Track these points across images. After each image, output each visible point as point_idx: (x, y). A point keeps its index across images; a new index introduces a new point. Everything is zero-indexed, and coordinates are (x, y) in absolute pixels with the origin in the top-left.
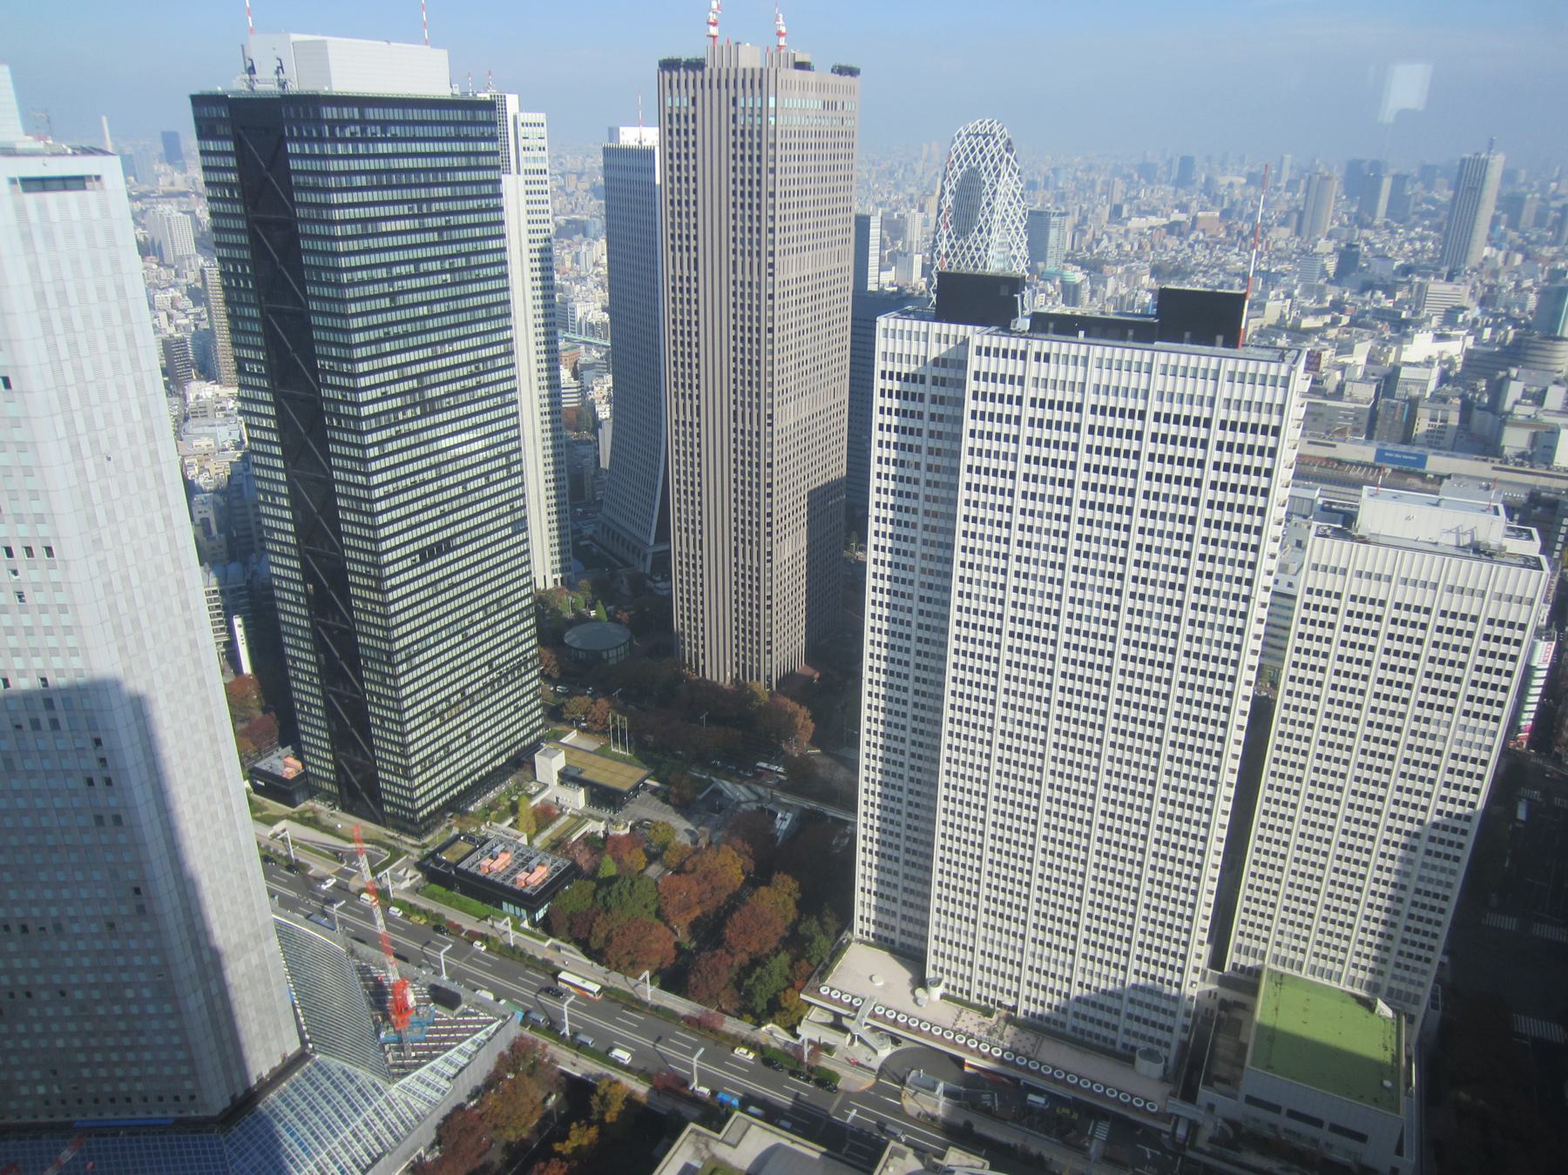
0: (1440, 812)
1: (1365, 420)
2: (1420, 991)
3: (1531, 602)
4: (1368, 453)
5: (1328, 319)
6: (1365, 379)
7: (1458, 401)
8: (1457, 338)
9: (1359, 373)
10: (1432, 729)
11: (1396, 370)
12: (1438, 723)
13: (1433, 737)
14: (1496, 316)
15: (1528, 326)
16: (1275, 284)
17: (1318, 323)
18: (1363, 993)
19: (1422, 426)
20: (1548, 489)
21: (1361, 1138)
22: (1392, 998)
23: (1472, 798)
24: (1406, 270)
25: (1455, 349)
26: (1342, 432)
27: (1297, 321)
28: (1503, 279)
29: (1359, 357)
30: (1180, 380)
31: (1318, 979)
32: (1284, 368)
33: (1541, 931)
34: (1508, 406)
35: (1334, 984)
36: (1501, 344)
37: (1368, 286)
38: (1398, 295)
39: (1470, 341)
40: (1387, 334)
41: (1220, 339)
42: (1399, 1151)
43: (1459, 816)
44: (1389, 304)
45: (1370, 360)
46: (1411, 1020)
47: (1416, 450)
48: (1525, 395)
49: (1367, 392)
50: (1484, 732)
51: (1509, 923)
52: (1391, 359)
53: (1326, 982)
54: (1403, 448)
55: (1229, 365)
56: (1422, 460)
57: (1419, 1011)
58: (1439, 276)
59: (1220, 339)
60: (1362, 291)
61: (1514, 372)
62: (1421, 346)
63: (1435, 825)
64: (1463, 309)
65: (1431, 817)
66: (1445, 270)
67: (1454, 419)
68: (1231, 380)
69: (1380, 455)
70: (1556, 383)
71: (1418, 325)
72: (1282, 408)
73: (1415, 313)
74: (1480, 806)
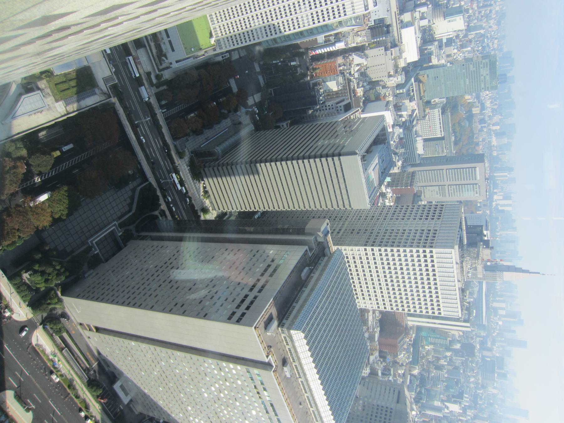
0: (278, 23)
2: (224, 48)
3: (354, 13)
10: (302, 7)
12: (305, 7)
13: (300, 9)
15: (447, 7)
18: (213, 34)
20: (393, 29)
21: (173, 50)
22: (218, 41)
23: (287, 30)
31: (209, 18)
33: (260, 78)
34: (418, 10)
35: (210, 24)
42: (177, 62)
43: (280, 29)
46: (214, 50)
48: (423, 13)
50: (308, 22)
51: (258, 69)
53: (210, 21)
57: (218, 51)
61: (430, 6)
63: (274, 25)
65: (275, 22)
70: (429, 21)
74: (286, 33)
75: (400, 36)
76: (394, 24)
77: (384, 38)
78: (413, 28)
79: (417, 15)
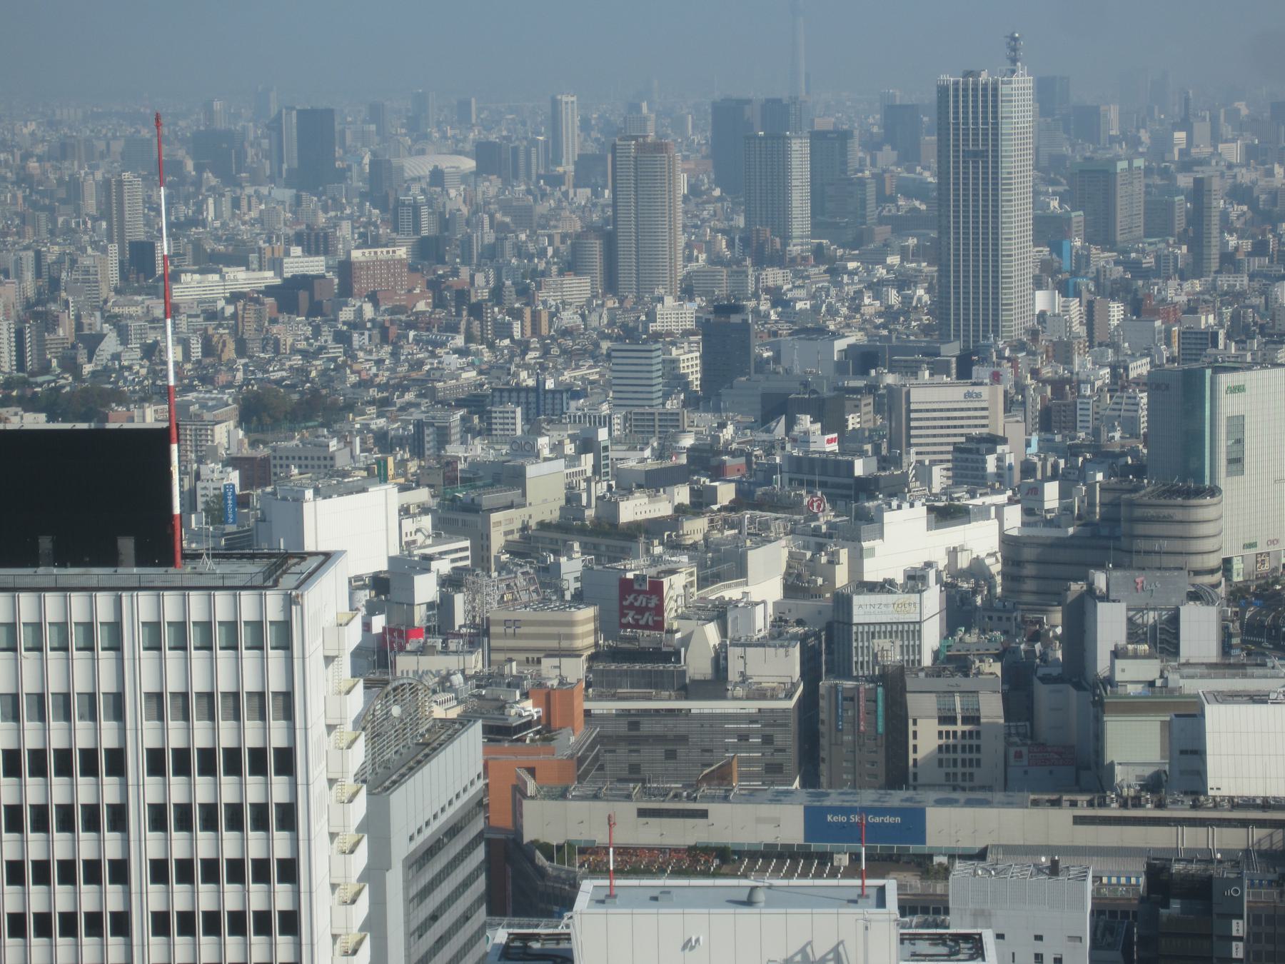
1: (788, 739)
4: (785, 823)
5: (682, 494)
6: (778, 633)
7: (997, 668)
8: (983, 513)
9: (761, 622)
11: (843, 603)
14: (1072, 452)
15: (1140, 470)
16: (557, 417)
17: (662, 508)
19: (926, 738)
24: (864, 359)
25: (980, 541)
26: (722, 776)
27: (609, 506)
28: (1082, 362)
29: (764, 582)
30: (54, 660)
32: (273, 601)
34: (1102, 664)
36: (1083, 519)
37: (777, 406)
38: (853, 421)
39: (1014, 518)
40: (826, 518)
41: (127, 545)
44: (827, 445)
45: (794, 586)
47: (897, 798)
48: (1135, 633)
49: (786, 665)
52: (842, 577)
54: (868, 797)
55: (142, 606)
56: (914, 823)
58: (939, 368)
59: (127, 545)
60: (765, 420)
61: (1100, 580)
62: (905, 540)
64: (993, 441)
66: (951, 350)
67: (992, 708)
68: (155, 645)
69: (814, 820)
70: (1195, 596)
71: (897, 491)
72: (287, 701)
73: (884, 463)
75: (1250, 810)
76: (1159, 838)
77: (1238, 927)
78: (1215, 716)
79: (1136, 673)
